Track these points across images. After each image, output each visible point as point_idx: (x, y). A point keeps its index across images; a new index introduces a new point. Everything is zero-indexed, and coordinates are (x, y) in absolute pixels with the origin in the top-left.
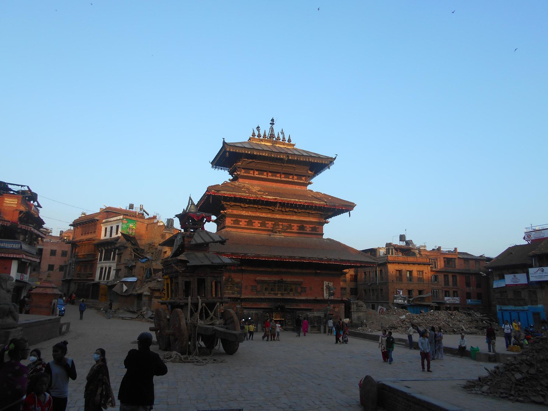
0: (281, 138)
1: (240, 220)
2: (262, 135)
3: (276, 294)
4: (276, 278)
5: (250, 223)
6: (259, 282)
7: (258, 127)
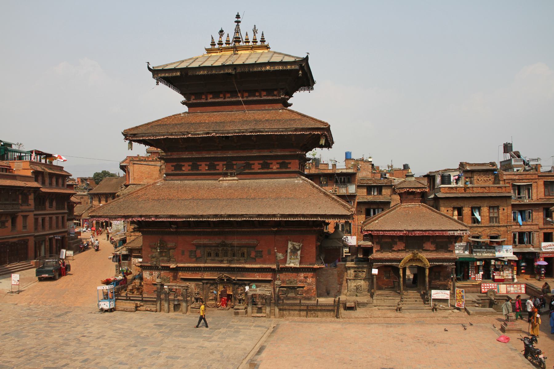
0: (251, 40)
1: (183, 164)
2: (224, 40)
3: (221, 262)
4: (217, 240)
5: (195, 167)
6: (198, 246)
7: (221, 31)
